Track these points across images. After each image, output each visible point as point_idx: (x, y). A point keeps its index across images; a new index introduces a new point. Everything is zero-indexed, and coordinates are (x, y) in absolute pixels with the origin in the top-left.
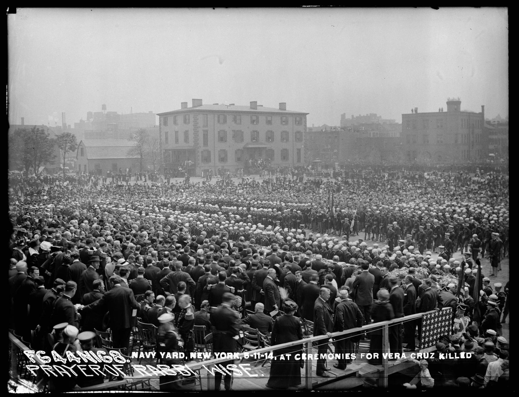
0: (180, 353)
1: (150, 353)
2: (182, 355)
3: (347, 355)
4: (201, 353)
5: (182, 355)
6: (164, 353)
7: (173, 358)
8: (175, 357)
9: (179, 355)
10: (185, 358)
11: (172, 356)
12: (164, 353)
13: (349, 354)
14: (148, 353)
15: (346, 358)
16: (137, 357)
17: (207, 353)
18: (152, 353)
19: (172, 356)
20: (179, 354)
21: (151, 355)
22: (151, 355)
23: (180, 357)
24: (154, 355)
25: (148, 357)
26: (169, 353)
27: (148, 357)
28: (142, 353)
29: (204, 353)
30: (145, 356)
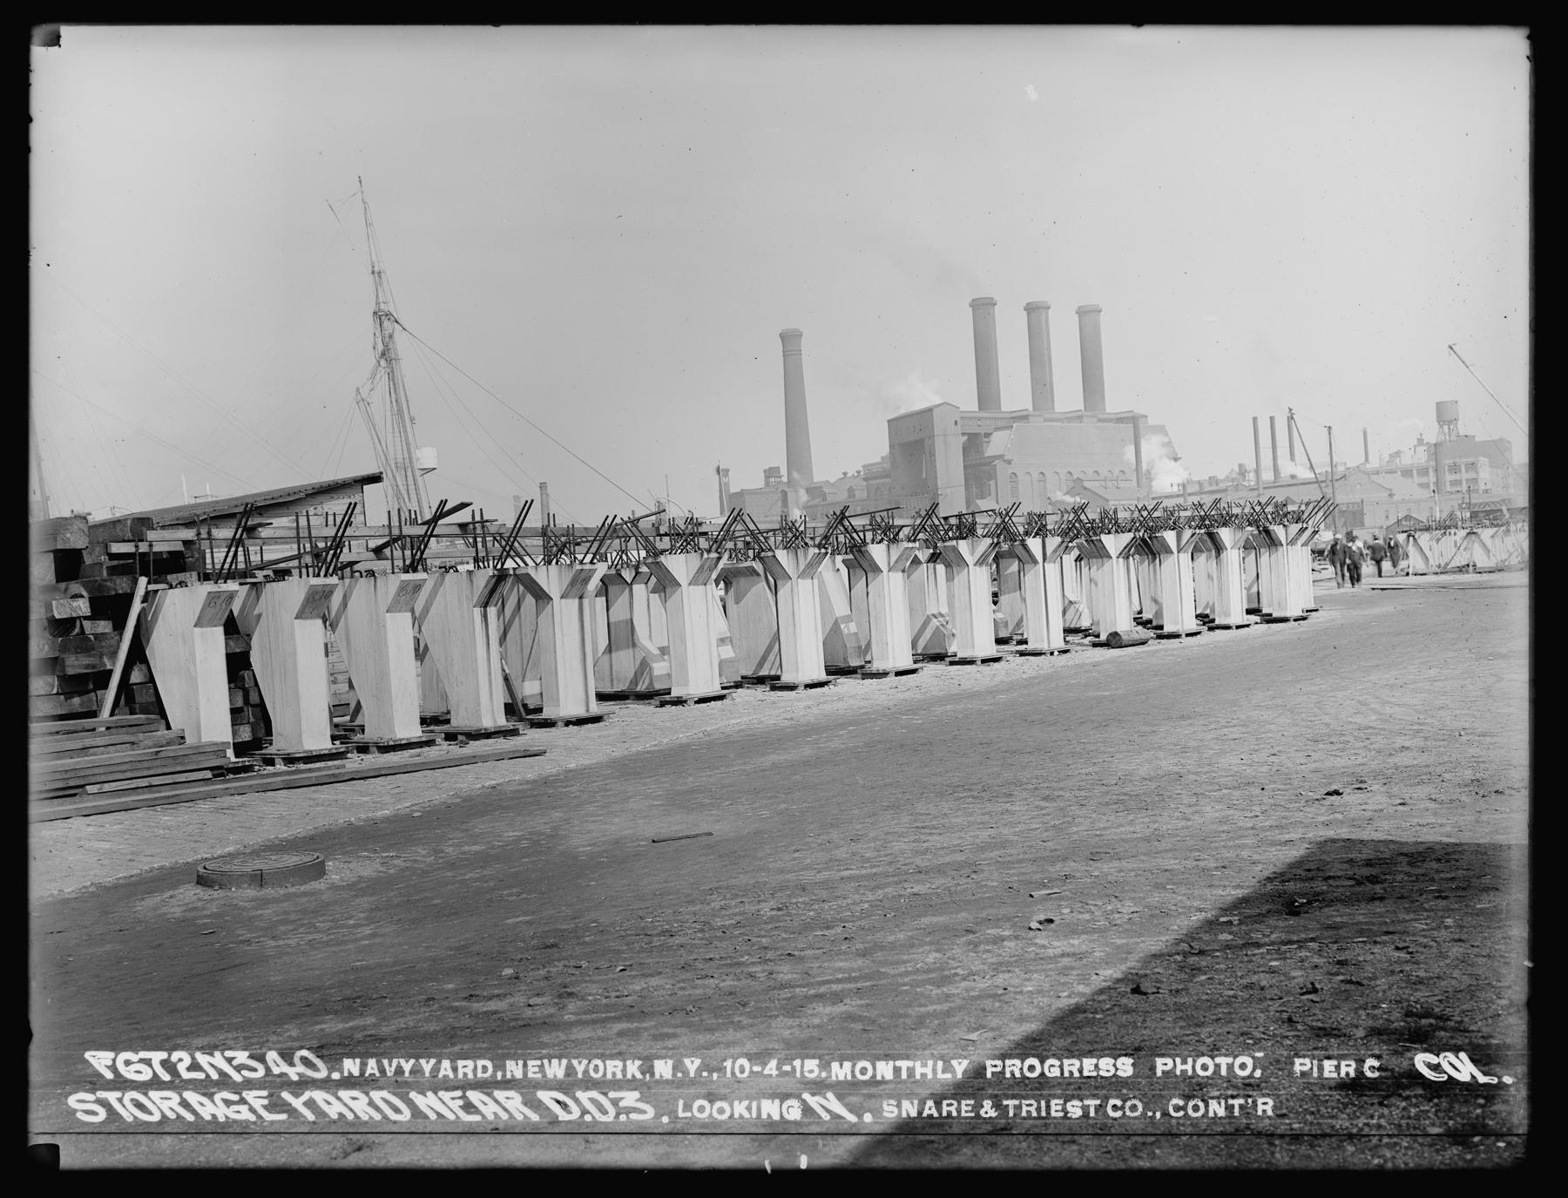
0: (480, 1063)
1: (395, 1062)
2: (485, 1068)
3: (1089, 1064)
4: (539, 1063)
5: (485, 1068)
6: (433, 1061)
7: (460, 1076)
8: (465, 1074)
9: (475, 1068)
10: (495, 1071)
11: (455, 1069)
12: (433, 1061)
13: (1094, 1061)
14: (390, 1066)
15: (1086, 1074)
16: (356, 1073)
17: (556, 1062)
18: (402, 1061)
19: (456, 1076)
20: (476, 1068)
21: (399, 1071)
22: (399, 1071)
23: (480, 1075)
24: (407, 1066)
25: (390, 1071)
26: (446, 1064)
27: (390, 1071)
28: (372, 1063)
29: (546, 1062)
30: (382, 1071)
